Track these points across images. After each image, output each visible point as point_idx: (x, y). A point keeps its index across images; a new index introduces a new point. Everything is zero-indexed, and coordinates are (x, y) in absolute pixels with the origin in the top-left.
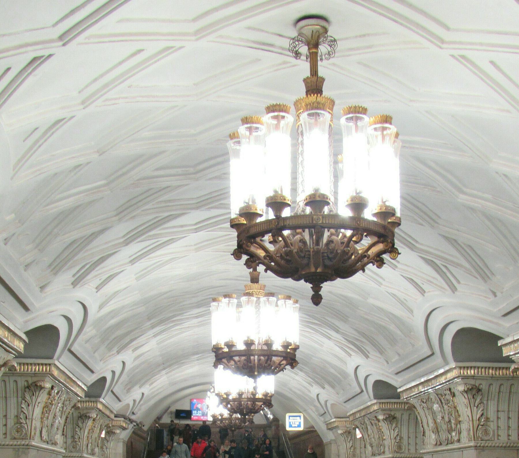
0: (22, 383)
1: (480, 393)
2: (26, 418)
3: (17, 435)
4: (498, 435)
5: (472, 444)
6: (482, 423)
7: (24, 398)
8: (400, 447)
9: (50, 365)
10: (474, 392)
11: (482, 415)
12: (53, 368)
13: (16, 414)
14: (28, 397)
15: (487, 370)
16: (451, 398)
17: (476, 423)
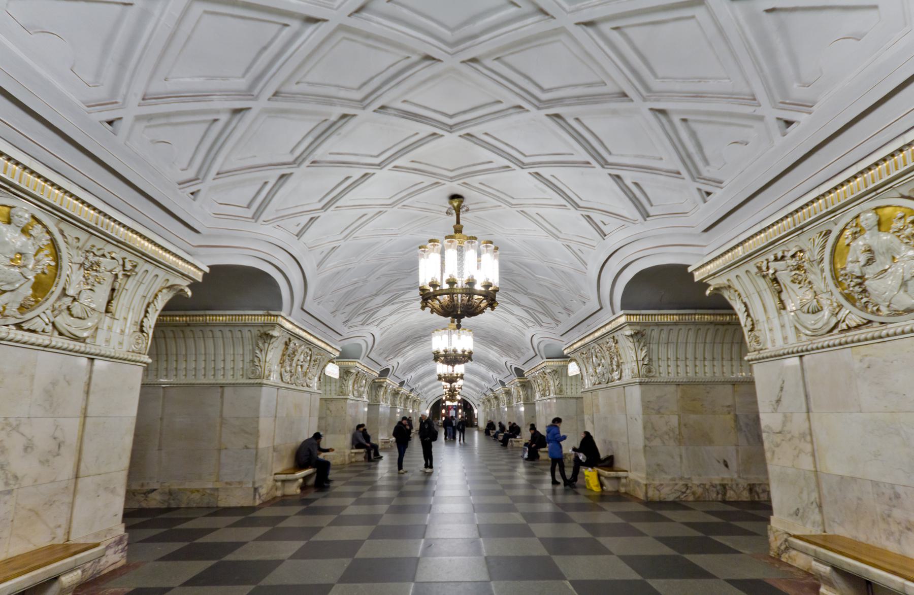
0: (255, 331)
1: (644, 337)
2: (260, 361)
3: (251, 376)
4: (660, 373)
5: (637, 380)
6: (646, 363)
7: (257, 345)
8: (561, 391)
9: (277, 316)
10: (639, 336)
11: (645, 356)
12: (280, 319)
13: (251, 358)
14: (261, 345)
15: (650, 317)
16: (614, 345)
17: (640, 363)
